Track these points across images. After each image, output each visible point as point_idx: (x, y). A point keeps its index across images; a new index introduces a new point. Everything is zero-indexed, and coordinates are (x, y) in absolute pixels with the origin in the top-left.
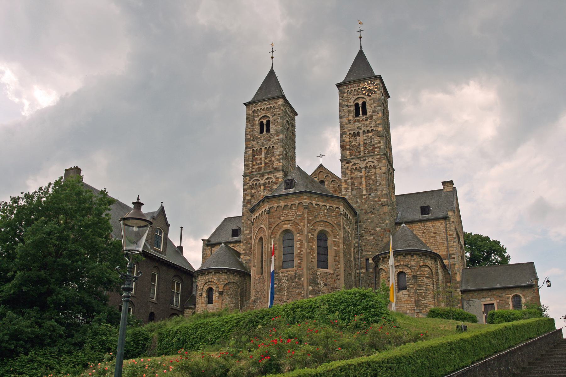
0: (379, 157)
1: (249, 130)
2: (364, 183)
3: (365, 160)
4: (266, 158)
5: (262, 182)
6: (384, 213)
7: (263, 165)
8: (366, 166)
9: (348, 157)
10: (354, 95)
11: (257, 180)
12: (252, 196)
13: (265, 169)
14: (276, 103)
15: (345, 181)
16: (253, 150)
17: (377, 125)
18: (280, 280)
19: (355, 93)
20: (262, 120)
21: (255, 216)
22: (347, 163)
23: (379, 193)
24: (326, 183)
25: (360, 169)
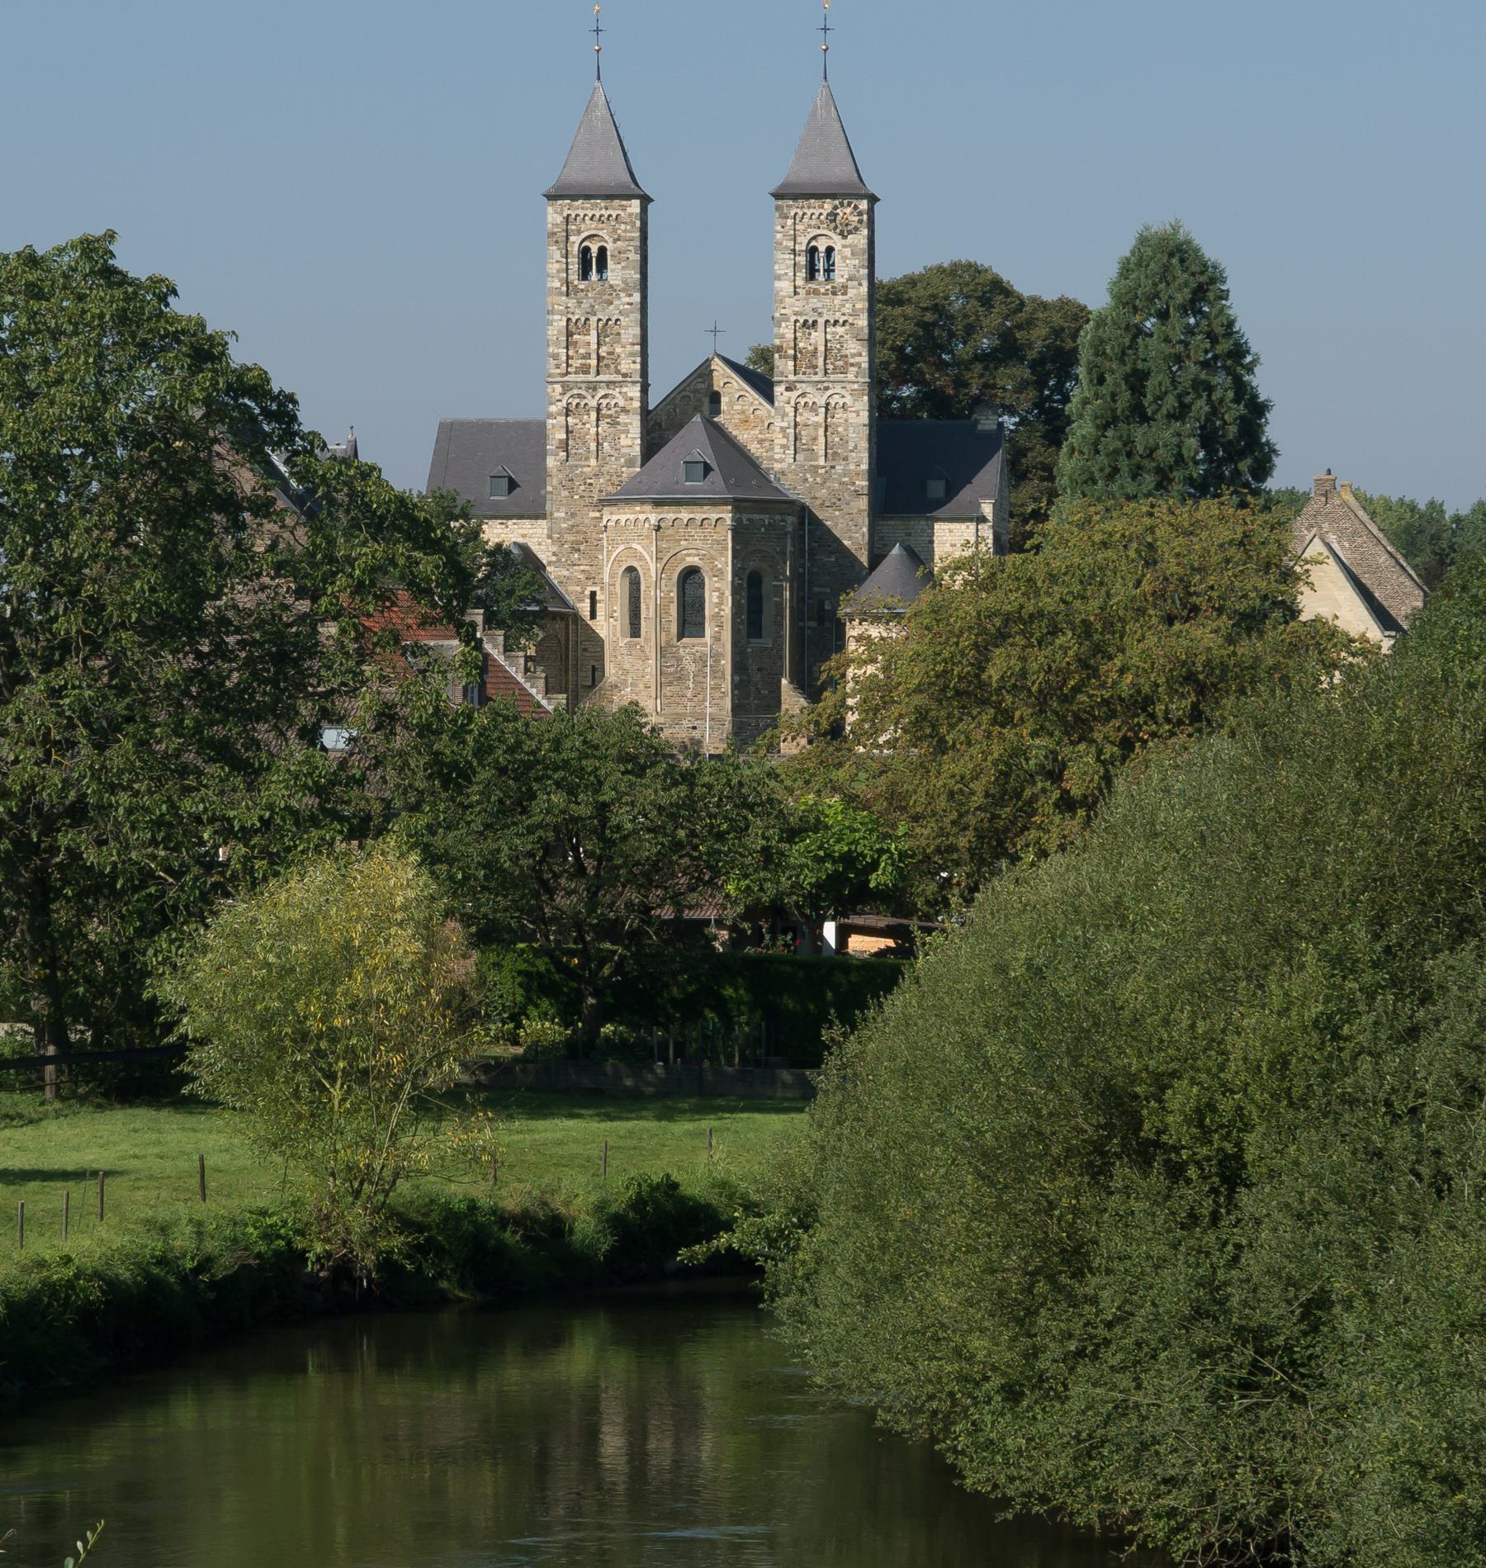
0: (856, 386)
1: (557, 266)
2: (822, 440)
3: (827, 389)
4: (599, 344)
5: (593, 403)
6: (860, 511)
7: (594, 362)
8: (828, 404)
9: (791, 377)
10: (810, 226)
11: (580, 396)
12: (568, 432)
13: (598, 373)
14: (624, 208)
15: (783, 430)
16: (569, 320)
17: (855, 314)
18: (679, 660)
19: (813, 223)
20: (586, 244)
21: (614, 518)
22: (788, 389)
23: (852, 467)
24: (724, 400)
25: (813, 408)
